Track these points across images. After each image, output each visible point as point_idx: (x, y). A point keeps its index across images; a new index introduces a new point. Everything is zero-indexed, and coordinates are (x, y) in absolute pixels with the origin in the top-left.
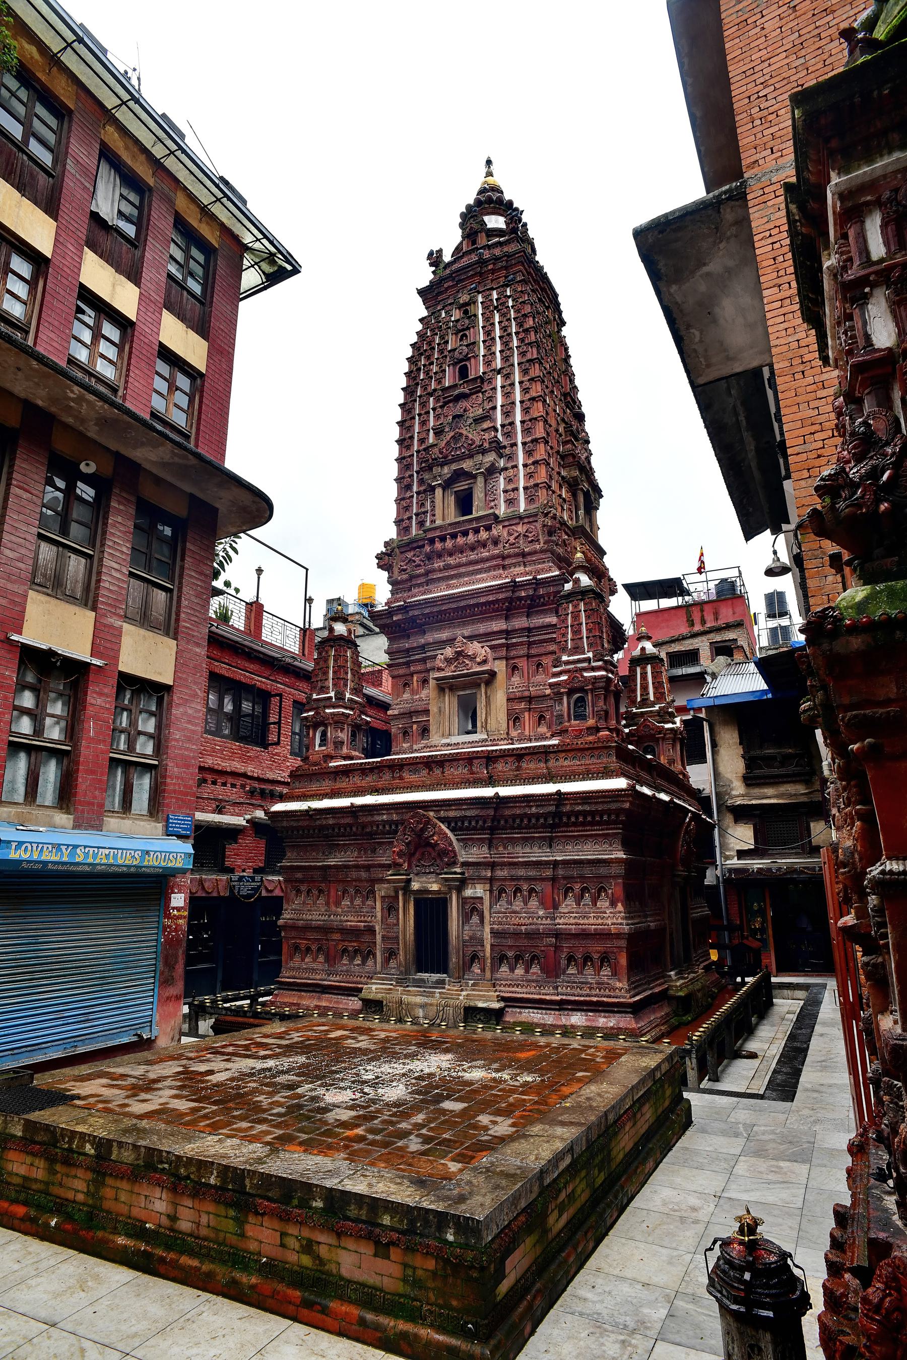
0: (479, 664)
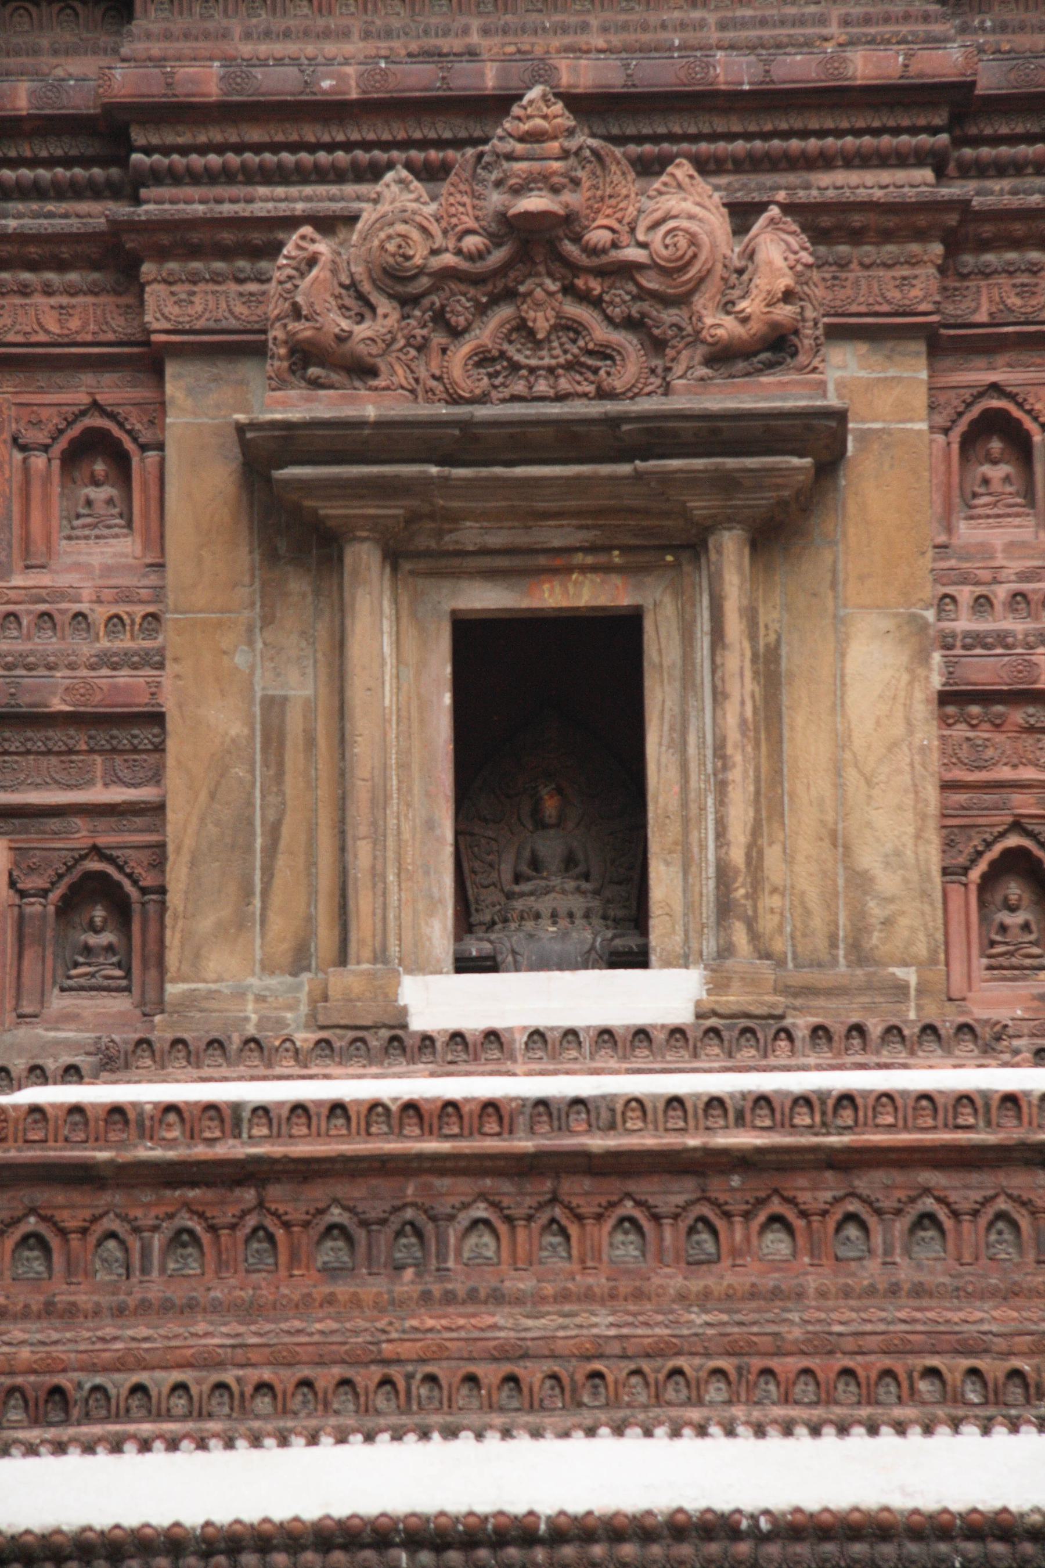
0: (723, 356)
